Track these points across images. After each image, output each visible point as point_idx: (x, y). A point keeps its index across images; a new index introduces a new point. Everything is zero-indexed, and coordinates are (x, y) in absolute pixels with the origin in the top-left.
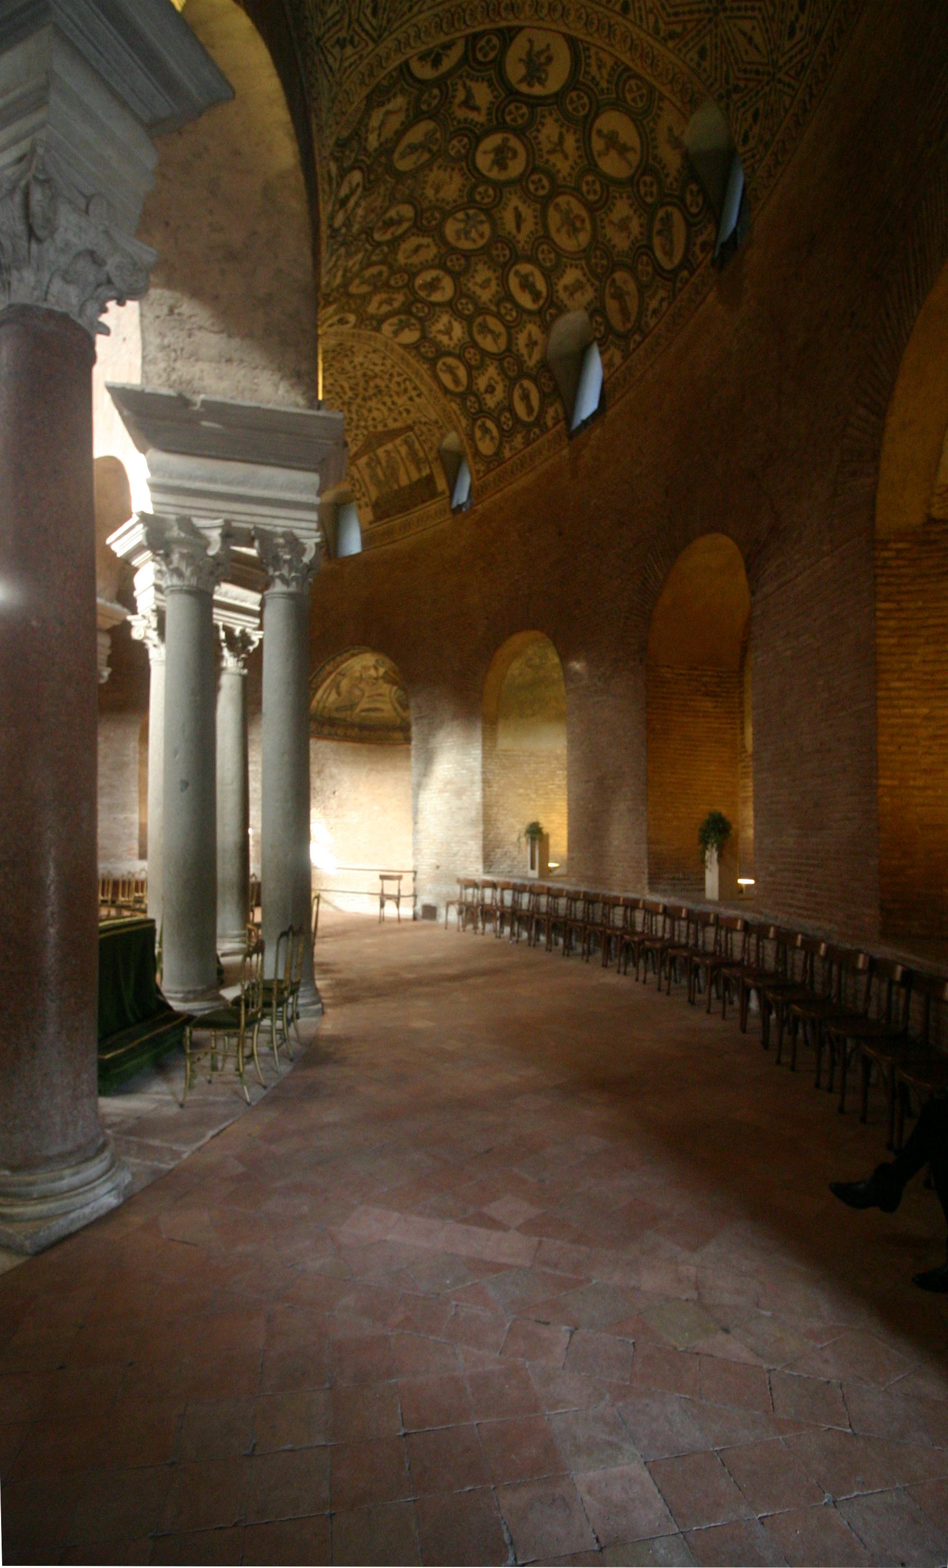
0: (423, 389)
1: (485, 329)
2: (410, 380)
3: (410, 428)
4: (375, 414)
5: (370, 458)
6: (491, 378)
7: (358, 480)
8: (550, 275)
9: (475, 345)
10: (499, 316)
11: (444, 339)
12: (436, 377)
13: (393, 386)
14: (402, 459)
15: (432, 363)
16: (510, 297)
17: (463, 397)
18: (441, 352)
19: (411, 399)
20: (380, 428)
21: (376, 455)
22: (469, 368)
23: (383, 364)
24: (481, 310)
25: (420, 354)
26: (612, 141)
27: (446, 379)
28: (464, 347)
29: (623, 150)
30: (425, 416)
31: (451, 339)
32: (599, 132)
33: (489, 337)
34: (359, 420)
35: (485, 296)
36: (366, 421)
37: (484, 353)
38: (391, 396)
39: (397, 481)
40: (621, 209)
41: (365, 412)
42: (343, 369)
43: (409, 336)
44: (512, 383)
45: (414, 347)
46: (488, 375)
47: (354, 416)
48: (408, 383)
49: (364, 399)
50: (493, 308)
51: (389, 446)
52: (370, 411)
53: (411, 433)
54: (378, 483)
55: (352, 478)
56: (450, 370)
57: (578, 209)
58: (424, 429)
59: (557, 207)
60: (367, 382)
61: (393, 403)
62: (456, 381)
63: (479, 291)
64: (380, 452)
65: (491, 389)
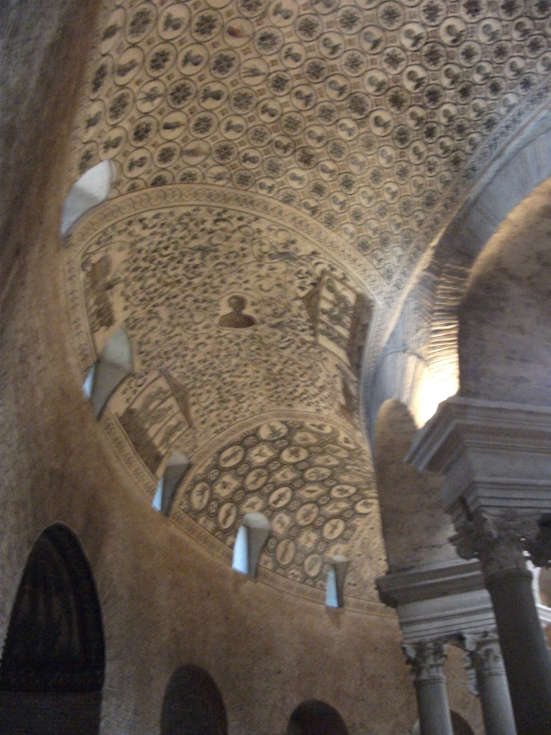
0: (220, 436)
1: (259, 476)
2: (228, 426)
3: (190, 426)
4: (204, 397)
5: (166, 392)
6: (230, 483)
7: (145, 380)
8: (285, 507)
9: (250, 470)
10: (265, 484)
11: (256, 451)
12: (231, 445)
13: (225, 413)
14: (167, 422)
15: (240, 443)
16: (276, 488)
17: (216, 466)
18: (247, 449)
19: (214, 425)
20: (192, 399)
21: (169, 397)
22: (235, 467)
23: (247, 411)
24: (270, 474)
25: (250, 436)
26: (335, 527)
27: (227, 453)
28: (249, 463)
29: (332, 532)
30: (201, 436)
31: (256, 455)
32: (337, 522)
33: (254, 478)
34: (201, 381)
35: (278, 476)
36: (200, 387)
37: (245, 476)
38: (218, 409)
39: (152, 425)
40: (314, 536)
41: (207, 388)
42: (257, 386)
43: (264, 433)
44: (230, 499)
45: (255, 433)
46: (232, 480)
47: (205, 378)
48: (227, 423)
49: (219, 389)
50: (271, 481)
51: (176, 409)
52: (208, 392)
53: (187, 426)
54: (145, 406)
55: (147, 373)
56: (234, 454)
57: (313, 516)
58: (190, 437)
59: (313, 508)
60: (235, 395)
61: (211, 411)
62: (227, 459)
63: (281, 473)
64: (171, 401)
65: (225, 486)
